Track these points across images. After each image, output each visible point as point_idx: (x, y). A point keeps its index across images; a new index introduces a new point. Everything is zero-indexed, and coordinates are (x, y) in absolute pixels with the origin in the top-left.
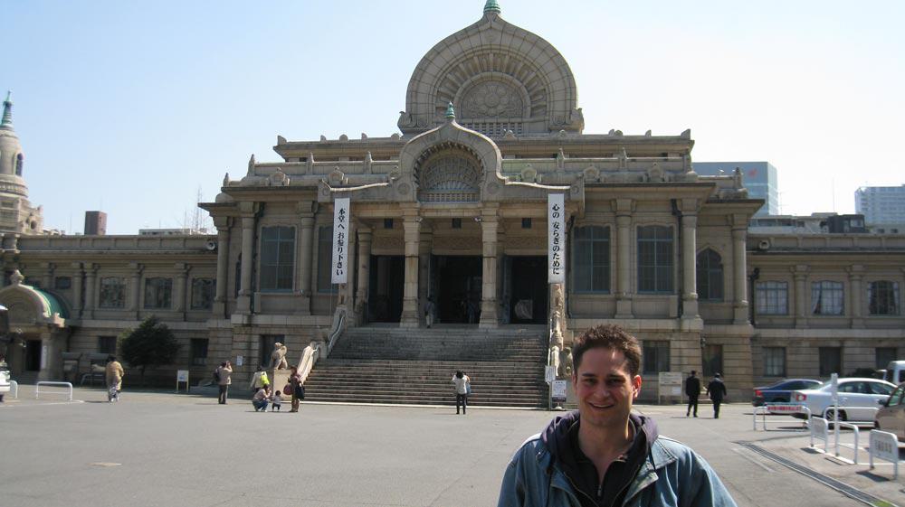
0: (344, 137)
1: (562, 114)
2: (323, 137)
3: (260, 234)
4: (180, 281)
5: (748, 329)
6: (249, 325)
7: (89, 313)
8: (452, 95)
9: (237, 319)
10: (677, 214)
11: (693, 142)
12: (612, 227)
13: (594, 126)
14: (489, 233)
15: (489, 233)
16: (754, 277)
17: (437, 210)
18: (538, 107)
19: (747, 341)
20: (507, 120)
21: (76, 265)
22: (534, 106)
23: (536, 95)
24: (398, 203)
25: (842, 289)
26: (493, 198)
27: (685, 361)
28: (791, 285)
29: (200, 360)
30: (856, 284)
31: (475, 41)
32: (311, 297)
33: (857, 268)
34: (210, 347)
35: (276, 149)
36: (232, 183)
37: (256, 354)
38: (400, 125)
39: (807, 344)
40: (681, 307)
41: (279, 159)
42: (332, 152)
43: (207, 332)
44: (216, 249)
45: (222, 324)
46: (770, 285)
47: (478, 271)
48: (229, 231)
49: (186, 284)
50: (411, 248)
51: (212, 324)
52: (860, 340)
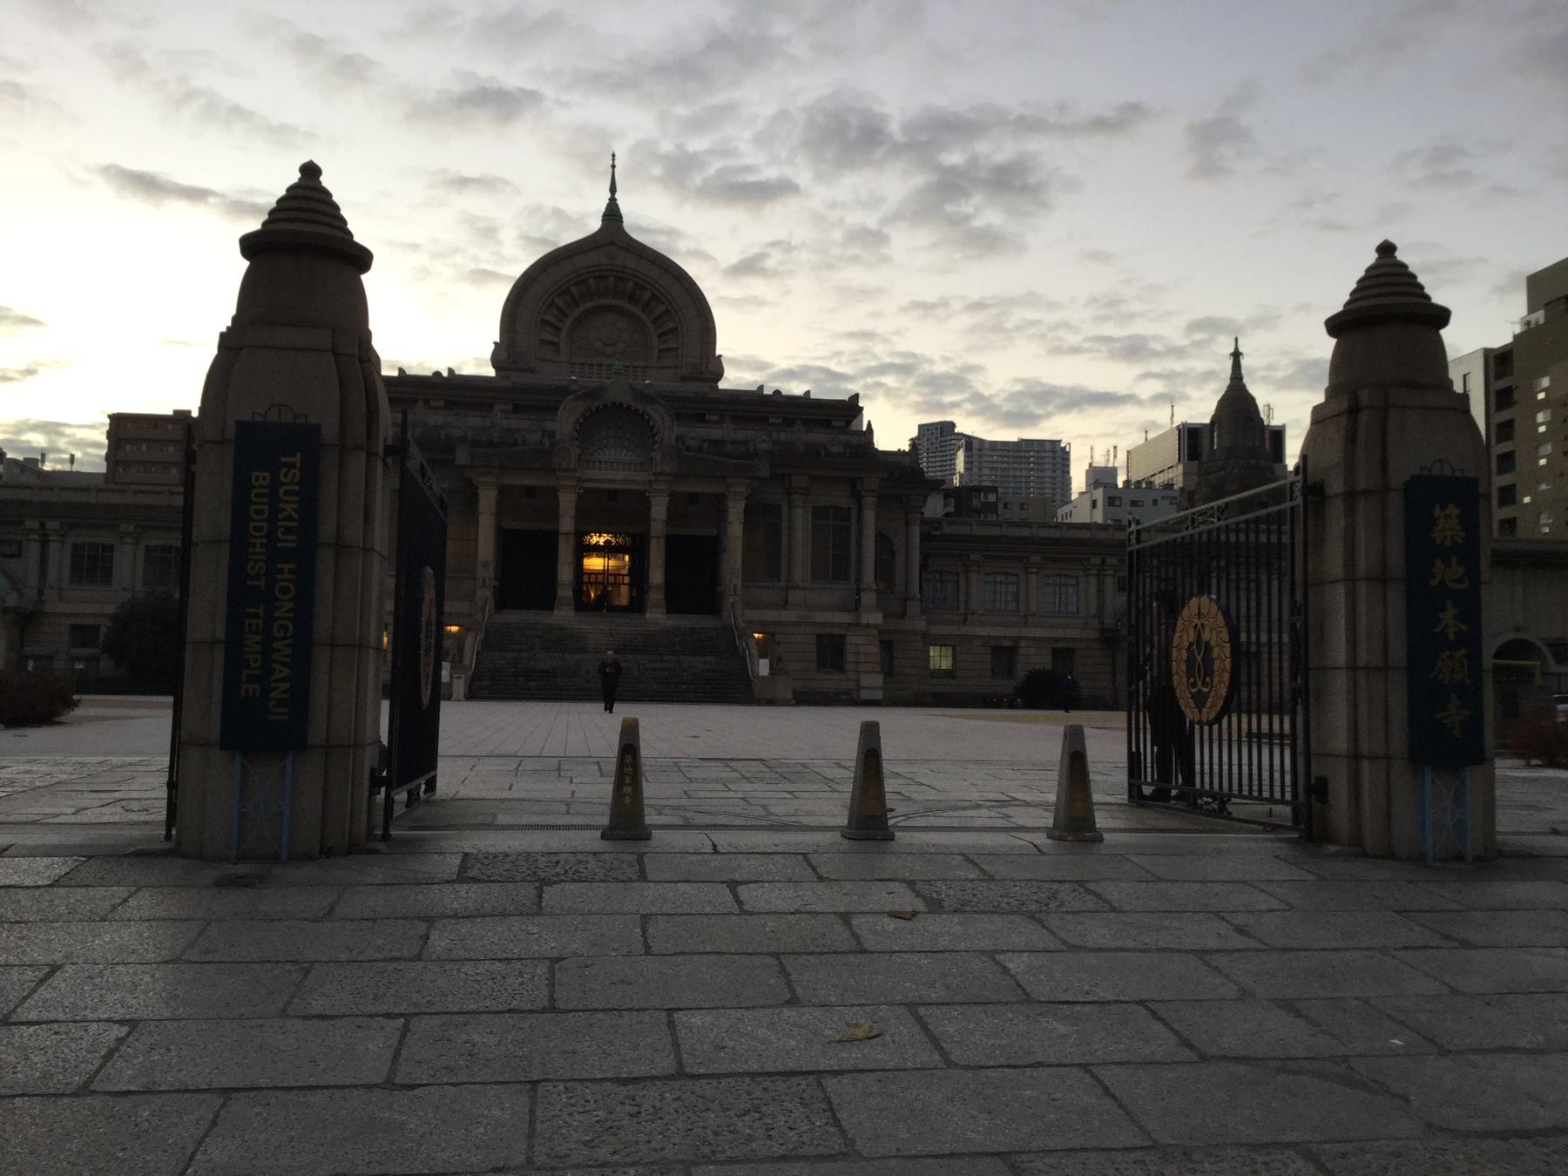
0: (437, 374)
2: (401, 370)
12: (785, 507)
14: (659, 510)
15: (659, 510)
17: (598, 481)
18: (668, 349)
21: (33, 524)
22: (663, 347)
23: (665, 333)
26: (667, 469)
28: (962, 576)
30: (1033, 577)
33: (1036, 558)
38: (496, 361)
40: (858, 601)
52: (1034, 638)
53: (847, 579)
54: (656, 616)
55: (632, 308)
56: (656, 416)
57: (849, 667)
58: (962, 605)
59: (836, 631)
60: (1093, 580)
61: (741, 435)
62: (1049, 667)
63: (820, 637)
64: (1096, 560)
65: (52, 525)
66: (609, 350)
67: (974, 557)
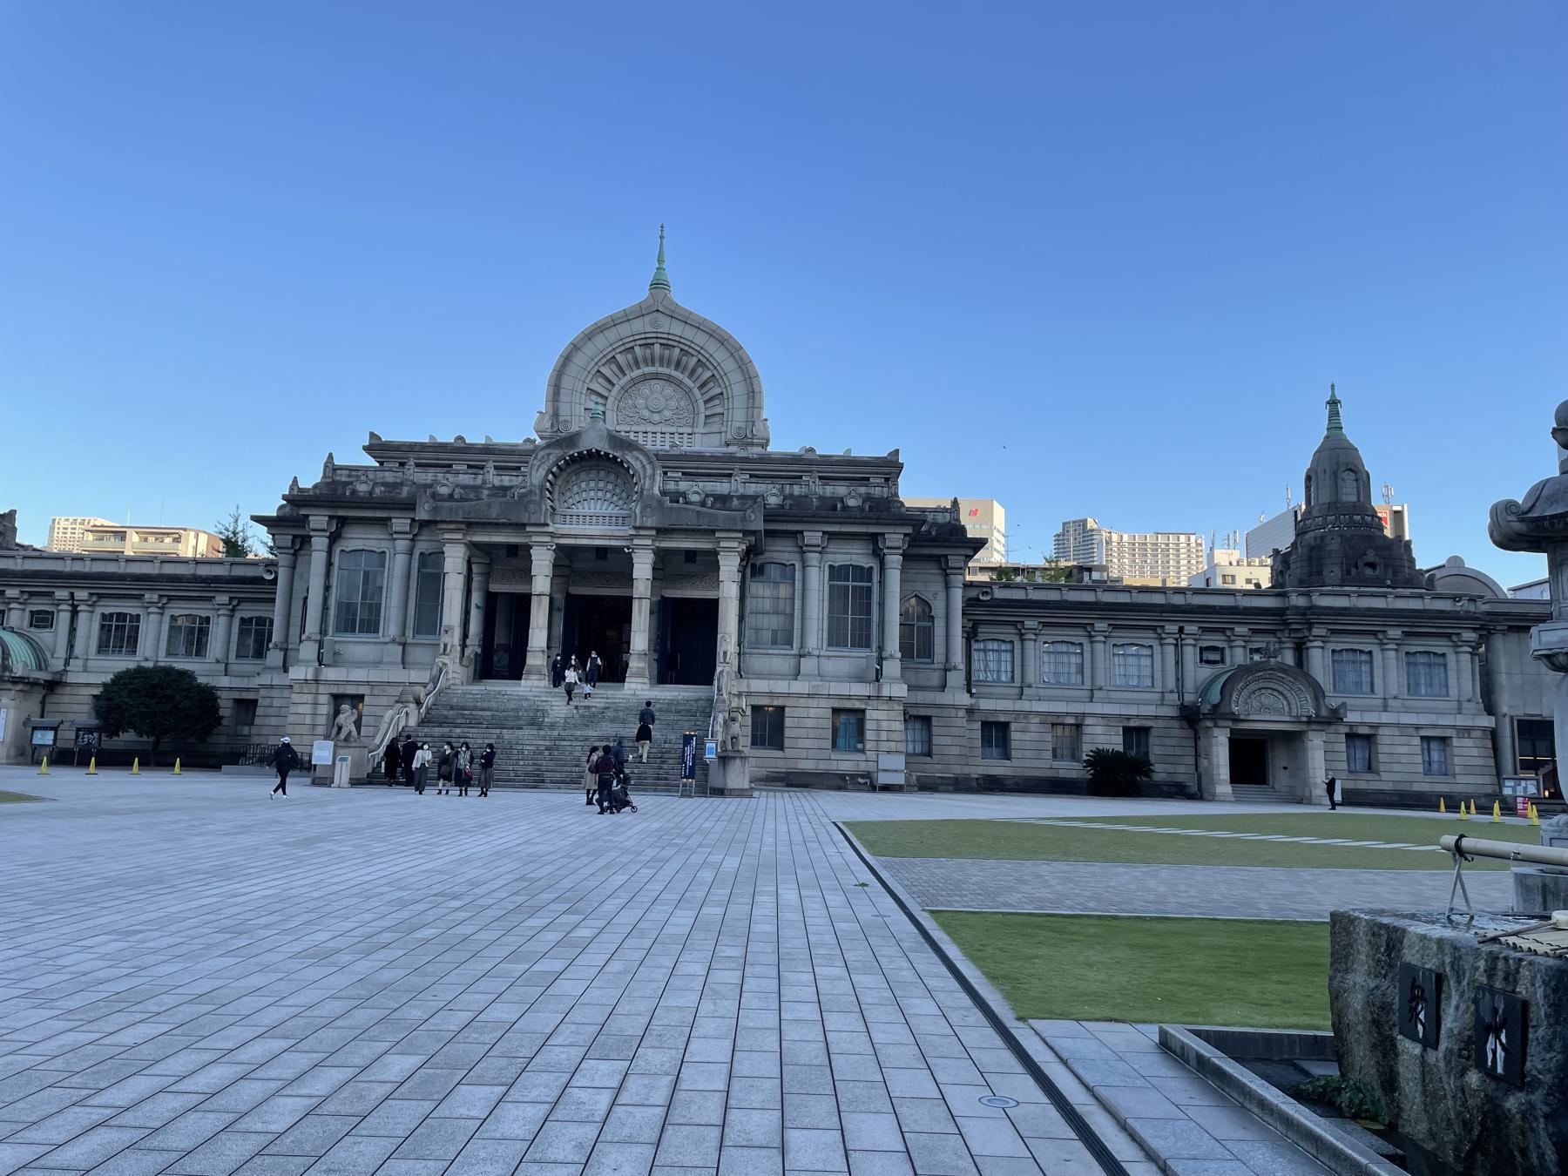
1: (742, 425)
3: (336, 560)
4: (223, 620)
5: (964, 699)
6: (316, 681)
7: (80, 663)
8: (605, 393)
9: (296, 673)
10: (879, 555)
11: (901, 467)
13: (783, 442)
14: (643, 568)
15: (643, 568)
16: (971, 635)
17: (575, 536)
19: (962, 713)
20: (673, 430)
24: (524, 525)
25: (1082, 654)
27: (884, 736)
28: (1017, 645)
29: (246, 730)
31: (638, 326)
32: (404, 645)
33: (1101, 625)
34: (259, 711)
35: (368, 449)
36: (301, 490)
37: (322, 720)
39: (1037, 720)
40: (879, 674)
41: (372, 463)
42: (445, 457)
43: (257, 690)
44: (276, 579)
45: (278, 679)
46: (990, 645)
47: (627, 618)
48: (295, 554)
49: (230, 625)
50: (541, 582)
51: (265, 679)
52: (1103, 716)
53: (868, 646)
54: (638, 686)
55: (677, 374)
56: (637, 465)
57: (869, 746)
58: (1017, 677)
59: (858, 705)
60: (1170, 650)
61: (752, 489)
62: (1120, 748)
63: (836, 711)
64: (1172, 628)
65: (81, 594)
66: (656, 417)
67: (1029, 623)
